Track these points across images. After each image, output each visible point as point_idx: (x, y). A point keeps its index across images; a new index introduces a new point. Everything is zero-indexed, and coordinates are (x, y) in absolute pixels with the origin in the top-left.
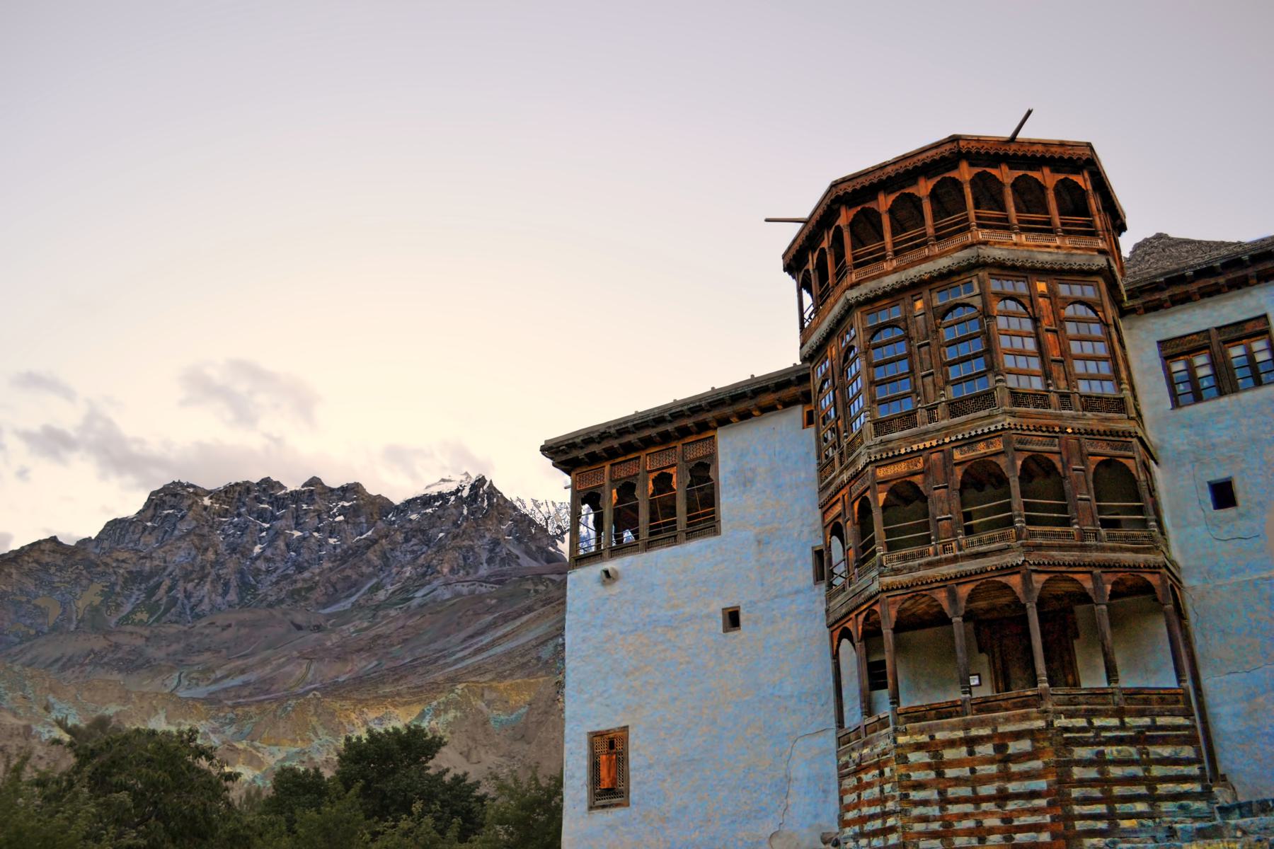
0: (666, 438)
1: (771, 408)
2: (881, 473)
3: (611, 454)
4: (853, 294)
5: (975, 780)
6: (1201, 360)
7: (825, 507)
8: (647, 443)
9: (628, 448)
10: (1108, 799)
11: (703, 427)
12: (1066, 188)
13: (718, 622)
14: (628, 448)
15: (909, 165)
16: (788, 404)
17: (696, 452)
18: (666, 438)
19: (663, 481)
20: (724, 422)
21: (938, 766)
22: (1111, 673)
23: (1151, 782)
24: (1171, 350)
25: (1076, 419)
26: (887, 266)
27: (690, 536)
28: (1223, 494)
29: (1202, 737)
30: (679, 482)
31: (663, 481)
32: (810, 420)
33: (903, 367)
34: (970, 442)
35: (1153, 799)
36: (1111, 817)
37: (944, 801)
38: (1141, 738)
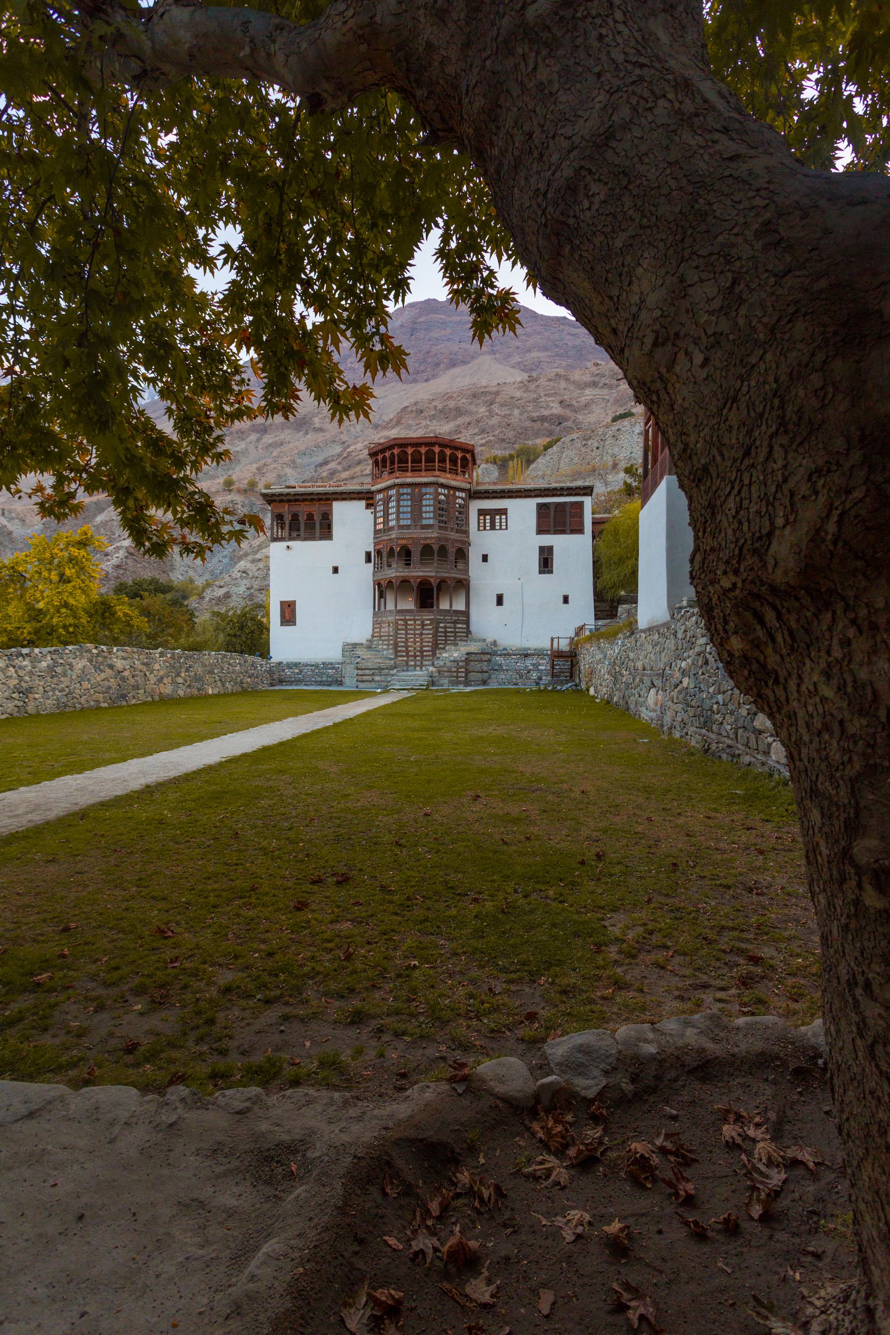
0: (312, 500)
1: (355, 499)
2: (400, 542)
3: (289, 501)
4: (398, 481)
5: (415, 629)
6: (488, 517)
7: (376, 544)
8: (304, 500)
9: (297, 500)
10: (446, 636)
11: (327, 499)
12: (464, 459)
13: (331, 570)
14: (297, 500)
15: (421, 441)
16: (360, 499)
17: (325, 508)
18: (312, 500)
19: (310, 517)
20: (337, 499)
21: (406, 625)
22: (451, 606)
23: (455, 632)
24: (482, 512)
25: (454, 535)
26: (409, 474)
27: (321, 539)
28: (485, 558)
29: (467, 623)
30: (317, 518)
31: (310, 517)
32: (368, 506)
33: (409, 509)
34: (426, 539)
35: (455, 637)
36: (446, 640)
37: (406, 634)
38: (455, 622)
